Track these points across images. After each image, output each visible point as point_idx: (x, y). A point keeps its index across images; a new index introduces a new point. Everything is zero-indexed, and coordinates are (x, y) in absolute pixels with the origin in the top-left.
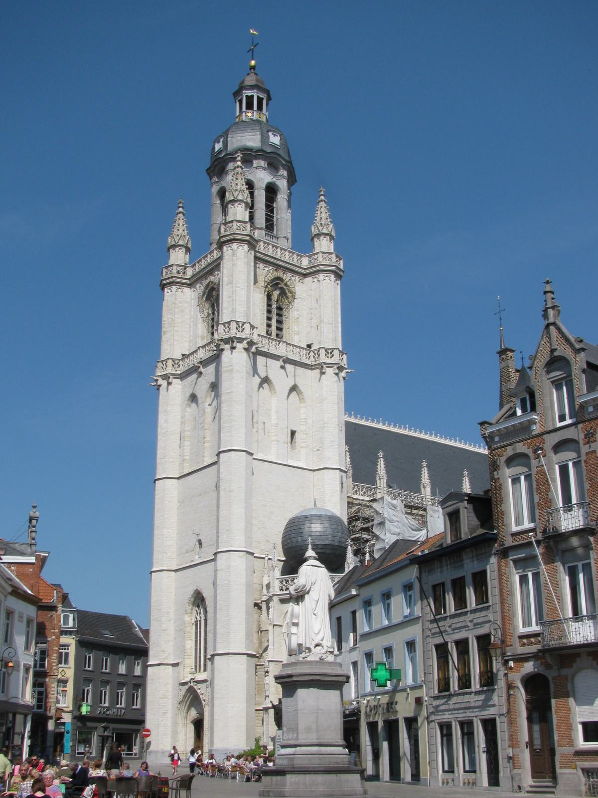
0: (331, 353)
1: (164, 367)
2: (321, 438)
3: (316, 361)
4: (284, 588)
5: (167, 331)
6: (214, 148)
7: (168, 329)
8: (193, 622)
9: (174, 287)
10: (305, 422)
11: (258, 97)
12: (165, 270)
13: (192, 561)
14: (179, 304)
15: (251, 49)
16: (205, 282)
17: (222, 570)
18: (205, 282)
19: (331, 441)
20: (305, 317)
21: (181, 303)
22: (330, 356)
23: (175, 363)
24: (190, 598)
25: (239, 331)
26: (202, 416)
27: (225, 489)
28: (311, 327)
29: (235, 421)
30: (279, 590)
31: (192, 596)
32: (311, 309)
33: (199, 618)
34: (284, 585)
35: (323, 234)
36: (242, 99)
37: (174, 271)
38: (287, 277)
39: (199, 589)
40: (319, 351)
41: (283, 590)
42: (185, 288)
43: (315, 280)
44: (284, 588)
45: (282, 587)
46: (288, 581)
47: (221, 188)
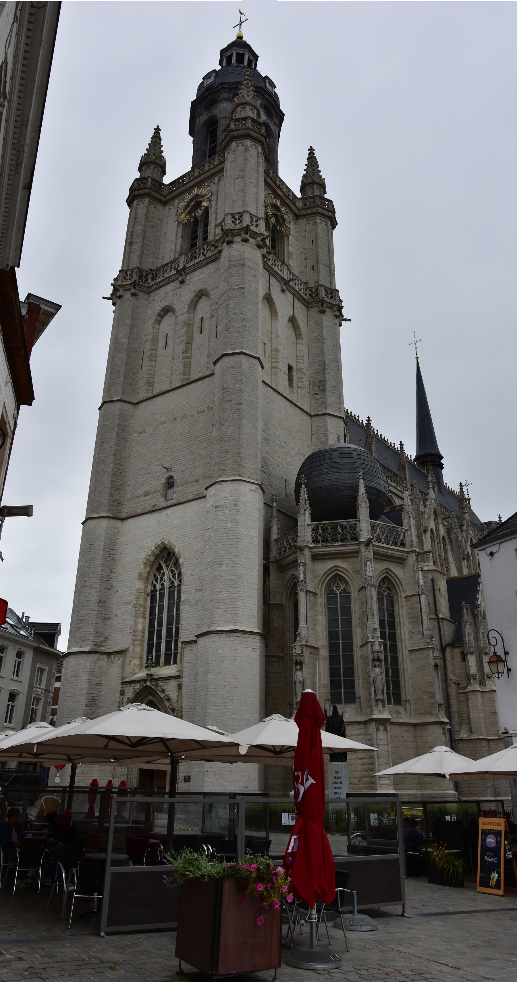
0: (331, 294)
1: (128, 278)
2: (320, 381)
3: (314, 299)
4: (320, 539)
5: (134, 242)
7: (135, 241)
8: (149, 591)
9: (146, 199)
10: (302, 359)
13: (155, 506)
14: (151, 219)
16: (188, 197)
17: (226, 506)
18: (188, 197)
19: (333, 386)
20: (298, 256)
21: (153, 218)
23: (143, 275)
24: (149, 556)
26: (181, 329)
27: (230, 401)
28: (306, 267)
30: (311, 541)
31: (153, 553)
32: (306, 249)
34: (320, 535)
35: (317, 183)
37: (149, 184)
38: (283, 209)
39: (166, 542)
40: (317, 289)
41: (318, 542)
42: (159, 205)
43: (311, 222)
44: (320, 539)
45: (317, 537)
46: (327, 529)
47: (210, 116)
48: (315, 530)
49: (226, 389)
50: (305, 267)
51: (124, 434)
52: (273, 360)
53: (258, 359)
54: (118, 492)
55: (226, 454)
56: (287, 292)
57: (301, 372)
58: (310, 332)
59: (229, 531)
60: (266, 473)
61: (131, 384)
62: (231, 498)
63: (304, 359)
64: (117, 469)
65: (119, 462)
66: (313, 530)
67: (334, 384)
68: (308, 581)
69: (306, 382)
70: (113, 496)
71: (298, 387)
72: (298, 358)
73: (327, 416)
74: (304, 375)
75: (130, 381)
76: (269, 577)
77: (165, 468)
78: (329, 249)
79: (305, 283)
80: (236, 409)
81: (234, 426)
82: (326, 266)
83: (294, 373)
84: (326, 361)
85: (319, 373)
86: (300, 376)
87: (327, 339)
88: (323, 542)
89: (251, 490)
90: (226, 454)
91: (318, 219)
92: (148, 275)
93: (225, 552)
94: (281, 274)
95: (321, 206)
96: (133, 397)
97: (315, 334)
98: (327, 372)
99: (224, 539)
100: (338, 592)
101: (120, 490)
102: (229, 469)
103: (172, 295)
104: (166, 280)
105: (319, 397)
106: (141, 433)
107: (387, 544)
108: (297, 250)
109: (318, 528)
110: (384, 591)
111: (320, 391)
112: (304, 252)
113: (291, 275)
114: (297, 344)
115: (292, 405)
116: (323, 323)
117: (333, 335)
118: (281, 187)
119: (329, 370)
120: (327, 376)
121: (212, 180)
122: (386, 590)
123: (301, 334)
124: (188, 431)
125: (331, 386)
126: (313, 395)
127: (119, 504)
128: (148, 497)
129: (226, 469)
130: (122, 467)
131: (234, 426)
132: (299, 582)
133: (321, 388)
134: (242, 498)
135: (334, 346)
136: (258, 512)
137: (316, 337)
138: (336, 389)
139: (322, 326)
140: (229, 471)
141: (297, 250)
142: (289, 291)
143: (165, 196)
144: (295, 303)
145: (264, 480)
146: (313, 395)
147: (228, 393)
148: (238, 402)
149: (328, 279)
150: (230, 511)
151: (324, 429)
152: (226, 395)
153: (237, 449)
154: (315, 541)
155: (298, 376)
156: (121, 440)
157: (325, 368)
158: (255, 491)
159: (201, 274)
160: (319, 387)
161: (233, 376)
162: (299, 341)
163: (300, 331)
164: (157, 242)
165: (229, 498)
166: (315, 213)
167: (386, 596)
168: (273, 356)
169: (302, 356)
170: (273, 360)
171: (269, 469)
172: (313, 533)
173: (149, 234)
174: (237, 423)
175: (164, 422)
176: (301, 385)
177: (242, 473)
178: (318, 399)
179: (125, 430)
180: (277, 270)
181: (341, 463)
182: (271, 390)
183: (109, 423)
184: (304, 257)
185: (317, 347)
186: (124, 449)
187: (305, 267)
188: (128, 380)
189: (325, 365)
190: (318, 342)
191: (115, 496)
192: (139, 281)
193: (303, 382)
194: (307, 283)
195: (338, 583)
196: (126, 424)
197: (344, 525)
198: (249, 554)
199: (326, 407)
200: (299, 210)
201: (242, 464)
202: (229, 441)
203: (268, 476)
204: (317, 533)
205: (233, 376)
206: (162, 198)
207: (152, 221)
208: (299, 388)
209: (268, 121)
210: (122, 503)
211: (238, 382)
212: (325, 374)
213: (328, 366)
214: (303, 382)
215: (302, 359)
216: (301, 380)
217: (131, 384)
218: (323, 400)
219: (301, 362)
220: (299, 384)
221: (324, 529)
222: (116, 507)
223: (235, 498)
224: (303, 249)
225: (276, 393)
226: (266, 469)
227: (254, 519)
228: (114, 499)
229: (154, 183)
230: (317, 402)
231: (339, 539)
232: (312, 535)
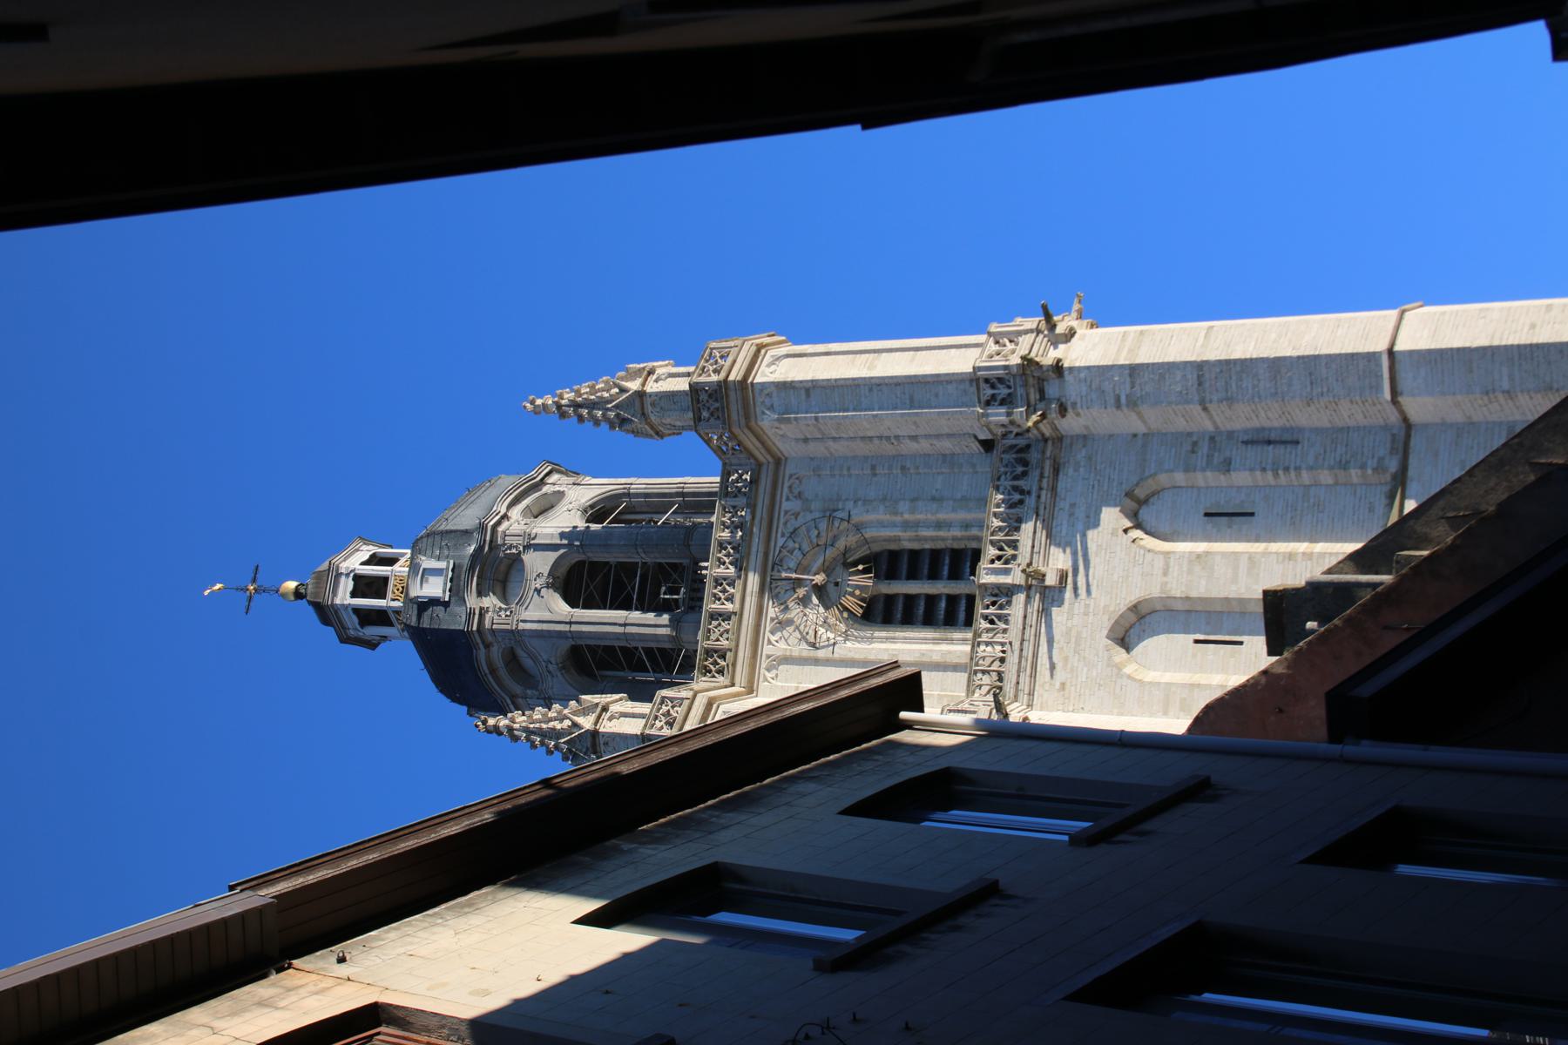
104: (1026, 637)
143: (733, 685)
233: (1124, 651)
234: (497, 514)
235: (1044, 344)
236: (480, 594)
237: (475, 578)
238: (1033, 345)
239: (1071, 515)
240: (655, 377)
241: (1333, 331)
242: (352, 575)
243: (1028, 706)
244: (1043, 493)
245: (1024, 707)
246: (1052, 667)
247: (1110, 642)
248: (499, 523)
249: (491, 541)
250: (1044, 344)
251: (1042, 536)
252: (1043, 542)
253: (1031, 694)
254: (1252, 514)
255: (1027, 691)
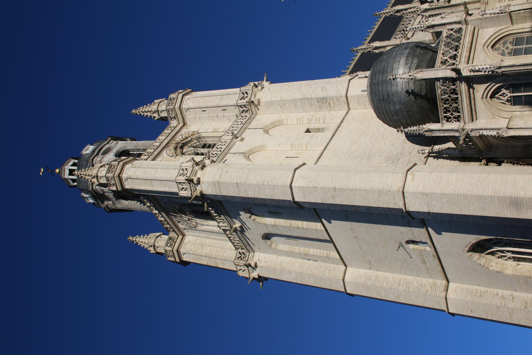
2: (318, 102)
4: (456, 114)
6: (93, 203)
10: (300, 119)
11: (72, 166)
12: (169, 259)
13: (434, 256)
15: (51, 173)
19: (322, 90)
20: (216, 123)
22: (246, 95)
25: (186, 174)
27: (333, 197)
29: (265, 181)
30: (458, 123)
33: (509, 255)
36: (71, 179)
37: (169, 249)
44: (456, 114)
45: (455, 118)
46: (445, 108)
48: (448, 119)
49: (322, 199)
50: (224, 117)
51: (373, 278)
52: (300, 149)
53: (296, 169)
54: (424, 286)
55: (380, 202)
56: (243, 136)
57: (311, 120)
58: (278, 112)
59: (451, 201)
60: (399, 158)
61: (330, 270)
62: (420, 200)
63: (300, 117)
64: (403, 285)
65: (397, 284)
66: (447, 121)
67: (320, 89)
68: (498, 127)
69: (320, 114)
70: (428, 290)
71: (324, 123)
72: (299, 123)
73: (348, 95)
74: (314, 118)
75: (327, 271)
76: (497, 158)
77: (399, 247)
78: (208, 96)
79: (237, 117)
80: (340, 192)
81: (354, 194)
82: (222, 98)
83: (311, 127)
84: (301, 97)
85: (311, 103)
86: (314, 121)
87: (282, 97)
88: (459, 112)
89: (413, 180)
90: (380, 202)
91: (184, 106)
92: (240, 253)
93: (472, 206)
94: (229, 142)
95: (174, 105)
96: (341, 268)
97: (279, 108)
98: (310, 97)
99: (459, 206)
100: (509, 95)
101: (422, 284)
102: (393, 200)
103: (253, 235)
104: (242, 240)
105: (332, 103)
106: (371, 264)
107: (461, 39)
108: (211, 124)
109: (445, 117)
110: (507, 48)
111: (327, 103)
112: (212, 118)
113: (229, 132)
114: (287, 124)
115: (339, 129)
116: (268, 101)
117: (278, 91)
118: (162, 141)
119: (308, 95)
120: (313, 97)
121: (160, 201)
122: (506, 46)
123: (279, 121)
124: (365, 227)
125: (322, 92)
126: (331, 109)
127: (434, 285)
128: (426, 261)
129: (394, 203)
130: (401, 281)
131: (354, 194)
132: (498, 136)
133: (325, 102)
134: (420, 189)
135: (287, 90)
136: (433, 173)
137: (281, 107)
138: (324, 87)
139: (271, 101)
140: (395, 200)
141: (211, 124)
142: (242, 133)
143: (178, 236)
144: (253, 127)
145: (405, 160)
146: (331, 109)
147: (326, 198)
148: (333, 190)
149: (232, 96)
150: (433, 200)
151: (360, 98)
152: (328, 200)
153: (375, 192)
154: (458, 119)
155: (315, 123)
156: (378, 281)
157: (307, 99)
158: (414, 176)
159: (233, 213)
160: (323, 103)
161: (311, 194)
162: (285, 123)
163: (276, 121)
164: (214, 243)
165: (421, 200)
166: (180, 110)
167: (513, 46)
168: (297, 149)
169: (298, 119)
170: (300, 149)
171: (397, 154)
172: (451, 121)
173: (208, 250)
174: (352, 191)
175: (359, 246)
176: (323, 120)
177: (396, 187)
178: (334, 104)
179: (369, 277)
180: (225, 146)
181: (384, 94)
182: (325, 152)
183: (363, 290)
184: (216, 118)
185: (289, 106)
186: (386, 278)
187: (224, 117)
188: (326, 273)
189: (304, 99)
190: (285, 105)
191: (428, 288)
192: (245, 261)
193: (319, 118)
194: (236, 115)
195: (501, 95)
196: (364, 276)
197: (441, 92)
198: (473, 183)
199: (340, 96)
200: (179, 123)
201: (388, 188)
202: (369, 199)
203: (402, 156)
204: (450, 118)
205: (311, 194)
206: (180, 237)
207: (198, 247)
208: (325, 122)
209: (113, 151)
210: (434, 282)
211: (315, 190)
212: (311, 98)
213: (304, 95)
214: (319, 118)
215: (300, 119)
216: (318, 120)
217: (330, 270)
218: (334, 99)
219: (303, 120)
220: (322, 121)
221: (446, 110)
222: (437, 287)
223: (420, 196)
224: (210, 119)
225: (328, 147)
226: (396, 158)
227: (440, 177)
228: (430, 289)
229: (169, 245)
230: (337, 104)
231: (455, 96)
232: (453, 122)
233: (269, 240)
234: (90, 185)
235: (193, 186)
236: (103, 203)
237: (99, 201)
238: (191, 188)
239: (233, 213)
240: (99, 178)
241: (273, 190)
242: (68, 169)
243: (254, 252)
244: (221, 210)
245: (253, 253)
246: (253, 244)
247: (264, 240)
248: (92, 187)
249: (94, 193)
250: (193, 186)
251: (228, 218)
252: (230, 219)
253: (252, 249)
254: (281, 213)
255: (251, 250)
